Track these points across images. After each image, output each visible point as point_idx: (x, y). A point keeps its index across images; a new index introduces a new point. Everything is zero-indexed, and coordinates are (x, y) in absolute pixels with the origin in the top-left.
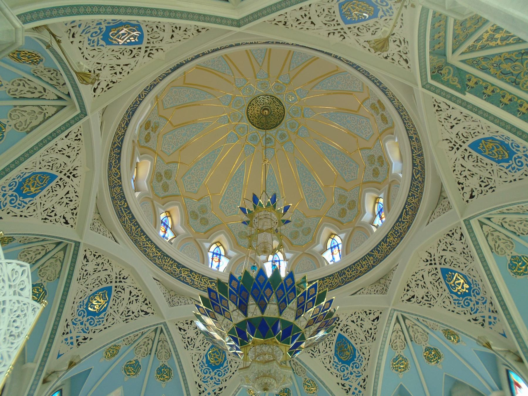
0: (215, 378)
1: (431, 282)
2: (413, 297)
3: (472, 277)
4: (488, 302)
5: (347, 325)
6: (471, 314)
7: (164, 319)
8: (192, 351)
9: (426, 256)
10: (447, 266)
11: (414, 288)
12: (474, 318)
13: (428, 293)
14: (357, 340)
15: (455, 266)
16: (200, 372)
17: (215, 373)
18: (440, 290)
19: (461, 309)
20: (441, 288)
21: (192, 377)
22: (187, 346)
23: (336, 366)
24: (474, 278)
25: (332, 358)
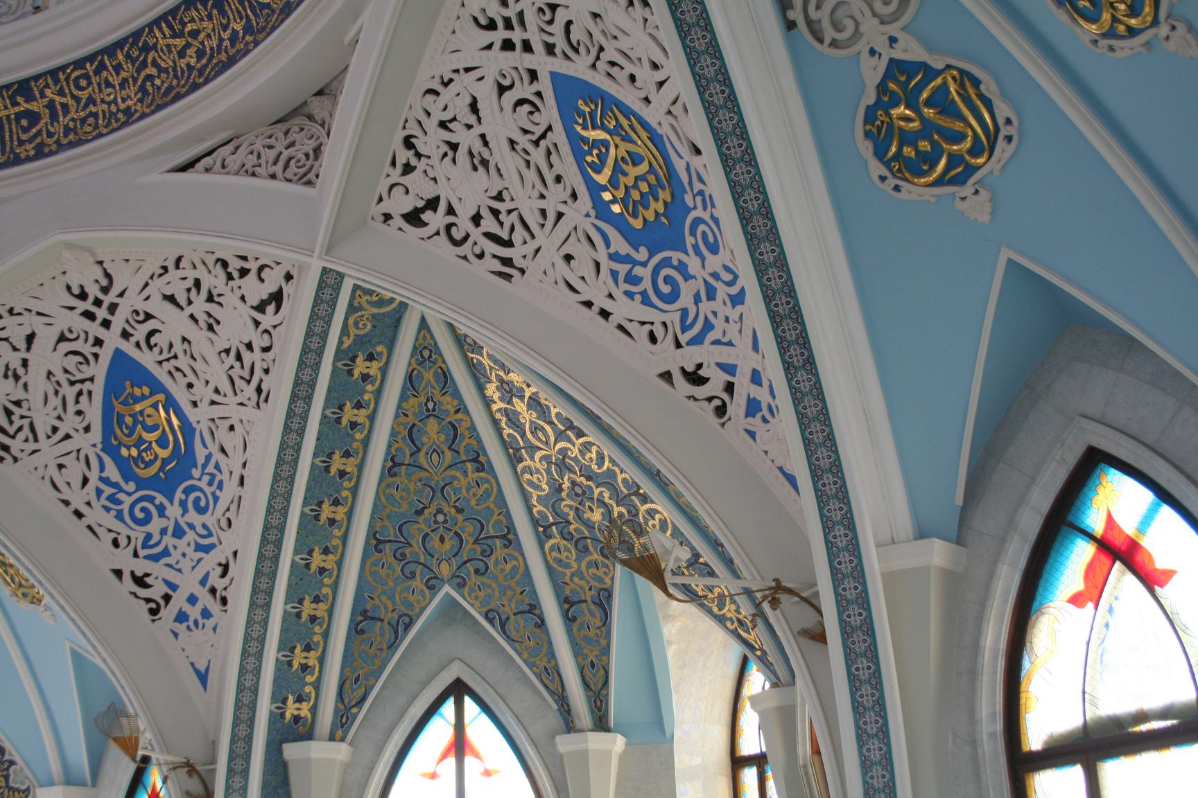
1: (50, 373)
3: (213, 448)
4: (217, 556)
6: (136, 555)
10: (147, 359)
12: (139, 573)
13: (18, 403)
15: (178, 375)
18: (70, 415)
19: (110, 520)
20: (79, 413)
24: (218, 456)
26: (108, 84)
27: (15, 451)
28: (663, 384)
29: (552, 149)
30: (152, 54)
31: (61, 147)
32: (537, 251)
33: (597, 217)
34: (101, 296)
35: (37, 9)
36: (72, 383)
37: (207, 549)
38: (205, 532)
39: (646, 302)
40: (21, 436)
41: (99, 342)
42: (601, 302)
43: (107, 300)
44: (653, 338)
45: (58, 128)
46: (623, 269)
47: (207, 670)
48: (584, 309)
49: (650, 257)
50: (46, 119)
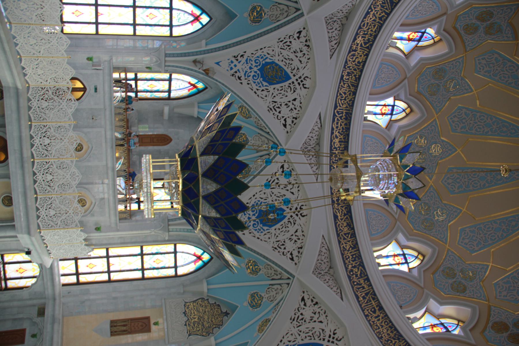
0: (251, 72)
1: (314, 328)
2: (305, 305)
5: (295, 224)
7: (308, 14)
8: (276, 47)
9: (339, 335)
11: (313, 308)
13: (305, 321)
14: (278, 232)
16: (256, 56)
17: (256, 72)
20: (306, 337)
21: (250, 48)
22: (281, 41)
23: (257, 203)
25: (265, 201)
26: (387, 330)
27: (293, 322)
30: (398, 341)
31: (369, 321)
34: (335, 339)
35: (401, 307)
36: (313, 334)
40: (297, 323)
41: (324, 340)
43: (334, 340)
45: (373, 319)
50: (375, 315)
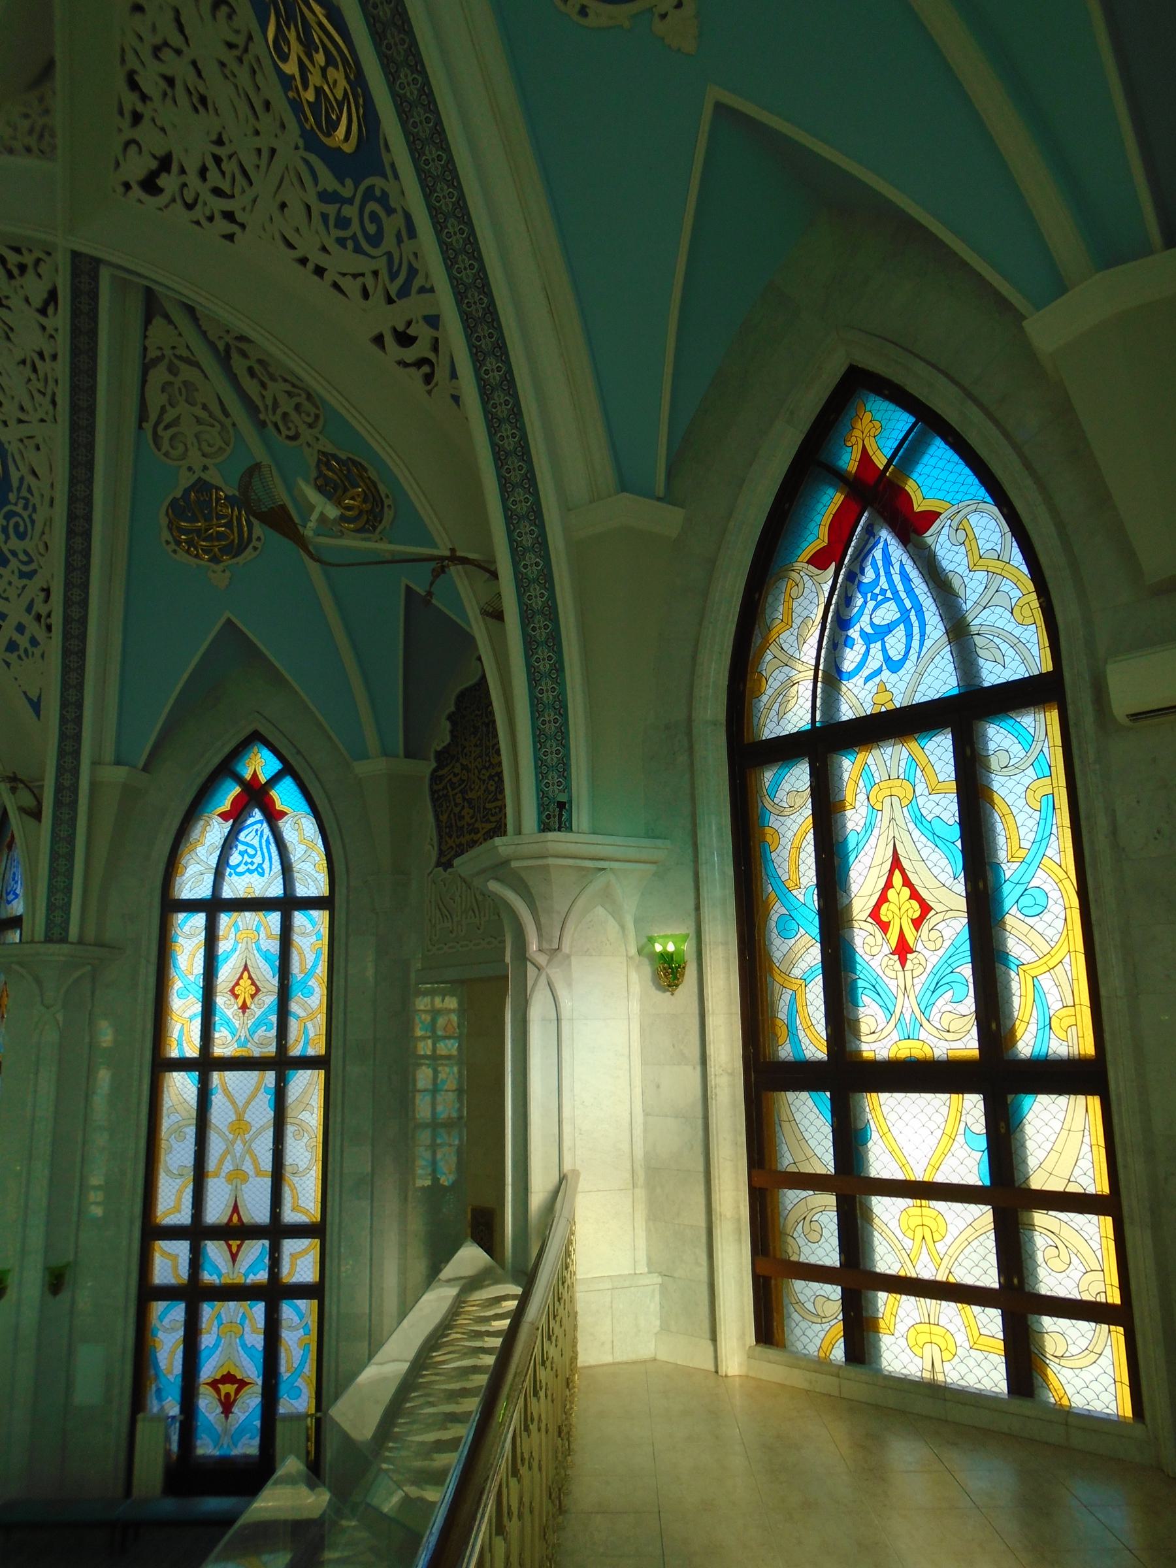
3: (24, 470)
4: (39, 581)
24: (30, 479)
28: (374, 348)
29: (256, 67)
32: (255, 201)
33: (306, 149)
37: (30, 575)
38: (25, 559)
39: (358, 250)
42: (316, 258)
44: (366, 295)
46: (331, 210)
47: (39, 697)
48: (299, 267)
49: (356, 188)
